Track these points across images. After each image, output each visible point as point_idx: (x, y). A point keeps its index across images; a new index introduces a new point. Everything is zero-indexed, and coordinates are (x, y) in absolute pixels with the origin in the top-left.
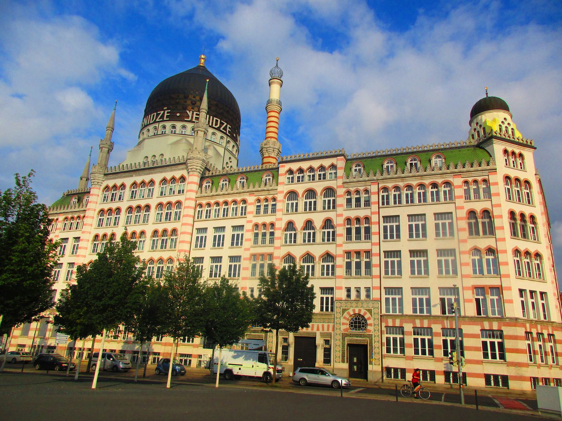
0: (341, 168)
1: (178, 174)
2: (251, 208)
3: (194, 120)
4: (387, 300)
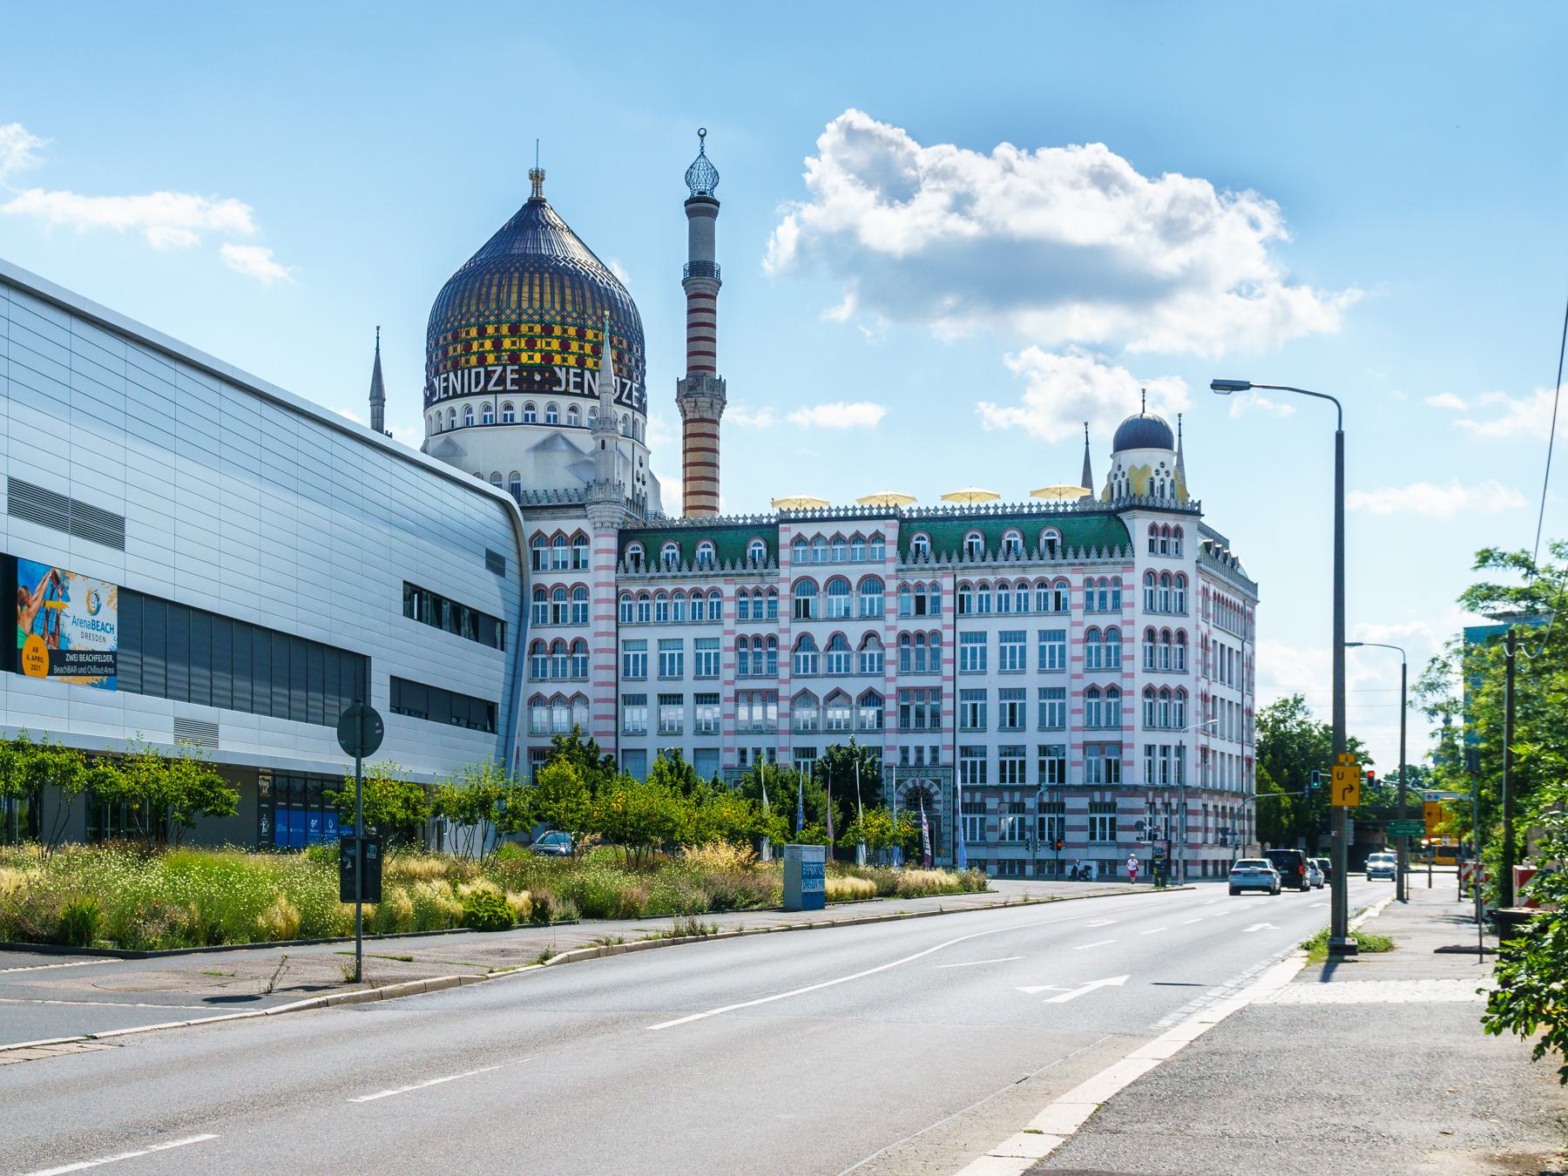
0: (891, 543)
1: (569, 527)
2: (729, 607)
3: (571, 389)
4: (964, 764)
